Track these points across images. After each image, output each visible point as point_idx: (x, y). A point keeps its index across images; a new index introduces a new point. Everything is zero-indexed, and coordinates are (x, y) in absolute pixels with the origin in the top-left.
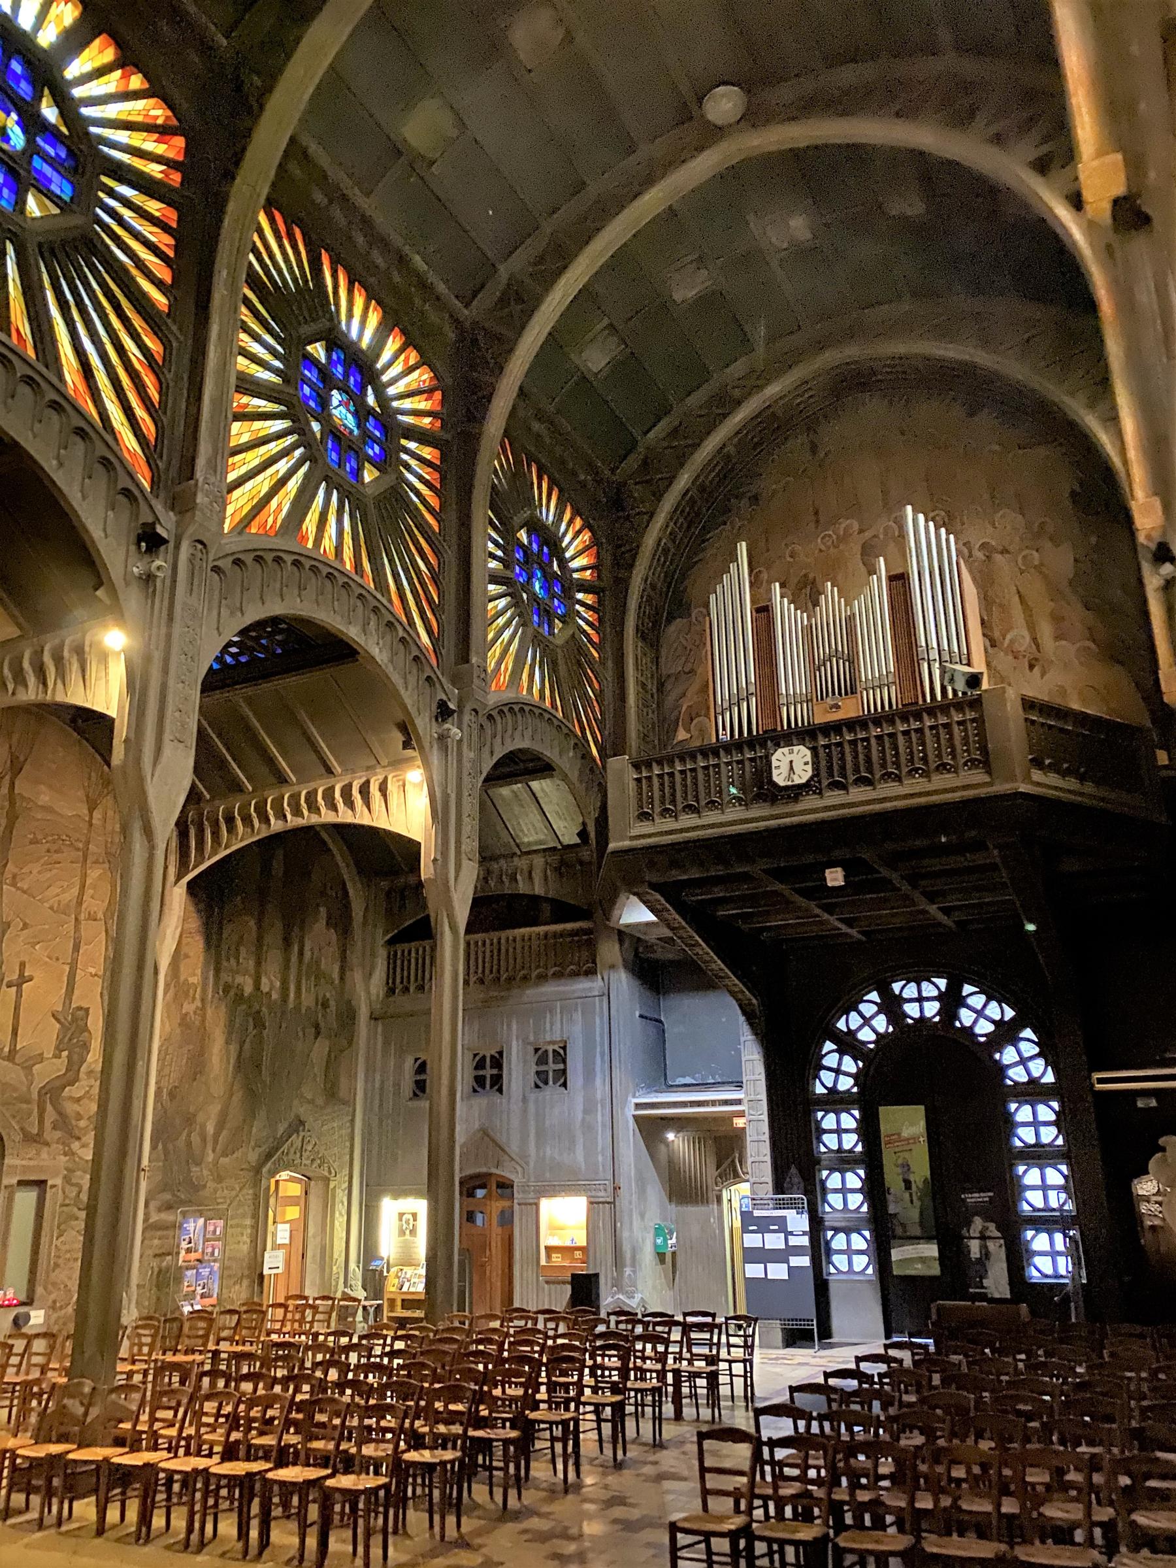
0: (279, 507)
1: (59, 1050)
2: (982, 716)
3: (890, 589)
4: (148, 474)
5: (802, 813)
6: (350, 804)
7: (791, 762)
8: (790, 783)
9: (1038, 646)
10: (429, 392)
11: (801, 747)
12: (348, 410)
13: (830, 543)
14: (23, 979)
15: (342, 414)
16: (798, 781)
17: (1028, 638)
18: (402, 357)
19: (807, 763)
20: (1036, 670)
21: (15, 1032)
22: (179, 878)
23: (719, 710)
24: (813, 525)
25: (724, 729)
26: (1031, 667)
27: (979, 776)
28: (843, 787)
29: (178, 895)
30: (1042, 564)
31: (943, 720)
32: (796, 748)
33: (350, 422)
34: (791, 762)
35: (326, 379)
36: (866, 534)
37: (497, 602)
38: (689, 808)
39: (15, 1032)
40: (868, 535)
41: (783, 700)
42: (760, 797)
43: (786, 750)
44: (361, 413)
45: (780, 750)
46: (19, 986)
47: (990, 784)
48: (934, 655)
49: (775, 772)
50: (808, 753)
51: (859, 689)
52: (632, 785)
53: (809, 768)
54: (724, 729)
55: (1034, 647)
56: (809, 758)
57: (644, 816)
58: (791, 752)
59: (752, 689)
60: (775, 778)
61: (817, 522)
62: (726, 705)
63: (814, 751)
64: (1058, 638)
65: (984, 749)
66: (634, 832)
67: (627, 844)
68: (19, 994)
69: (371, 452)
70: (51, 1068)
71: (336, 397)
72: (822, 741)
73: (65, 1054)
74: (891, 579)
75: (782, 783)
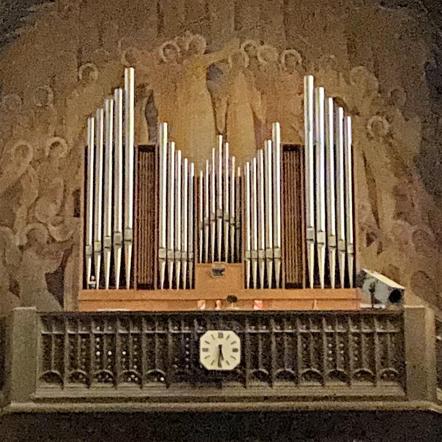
2: (402, 331)
3: (283, 159)
5: (223, 400)
7: (220, 347)
8: (217, 368)
9: (377, 220)
11: (231, 333)
13: (172, 57)
16: (225, 367)
17: (369, 209)
19: (235, 350)
20: (374, 246)
23: (88, 251)
24: (153, 31)
25: (93, 273)
26: (369, 241)
27: (394, 389)
28: (267, 379)
30: (390, 135)
31: (366, 330)
32: (226, 333)
34: (220, 347)
36: (213, 55)
38: (103, 378)
40: (213, 59)
41: (162, 255)
42: (181, 377)
43: (216, 333)
45: (209, 333)
47: (407, 400)
48: (321, 238)
49: (202, 355)
50: (238, 340)
51: (243, 259)
52: (40, 339)
53: (238, 355)
54: (93, 273)
55: (373, 219)
56: (238, 345)
57: (49, 378)
58: (221, 336)
59: (129, 235)
60: (202, 360)
61: (160, 28)
62: (97, 248)
63: (242, 336)
64: (399, 215)
65: (401, 366)
66: (39, 394)
67: (33, 405)
72: (250, 329)
74: (285, 149)
75: (209, 367)
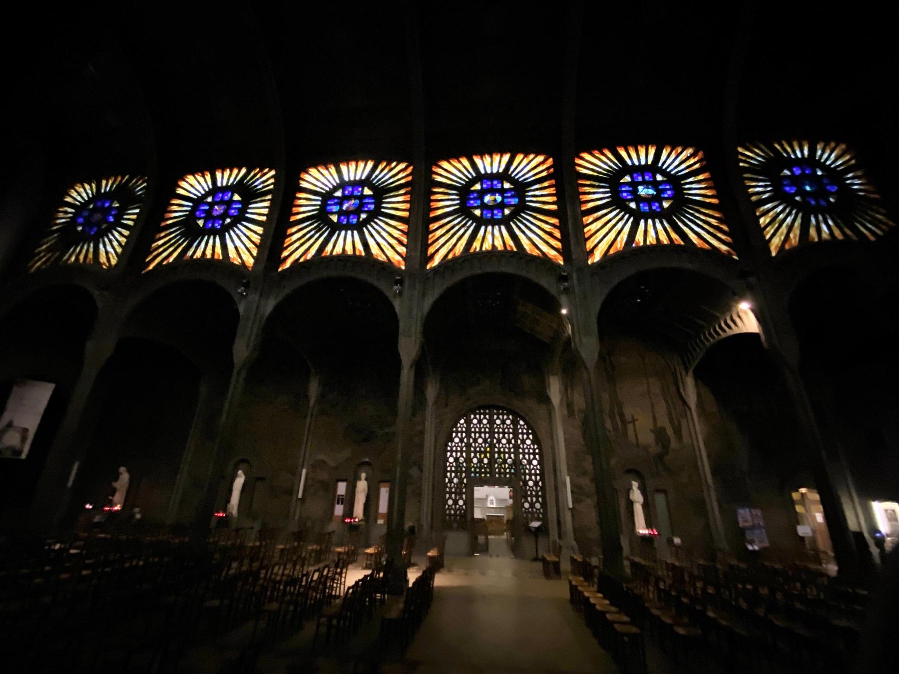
0: (622, 239)
1: (657, 443)
4: (561, 258)
6: (729, 327)
10: (693, 155)
12: (650, 188)
14: (634, 421)
15: (643, 191)
18: (674, 152)
21: (636, 436)
22: (687, 372)
29: (690, 382)
33: (651, 192)
35: (634, 185)
37: (775, 210)
39: (636, 436)
44: (655, 184)
46: (634, 423)
68: (634, 425)
69: (666, 196)
70: (655, 449)
71: (640, 188)
73: (660, 444)
